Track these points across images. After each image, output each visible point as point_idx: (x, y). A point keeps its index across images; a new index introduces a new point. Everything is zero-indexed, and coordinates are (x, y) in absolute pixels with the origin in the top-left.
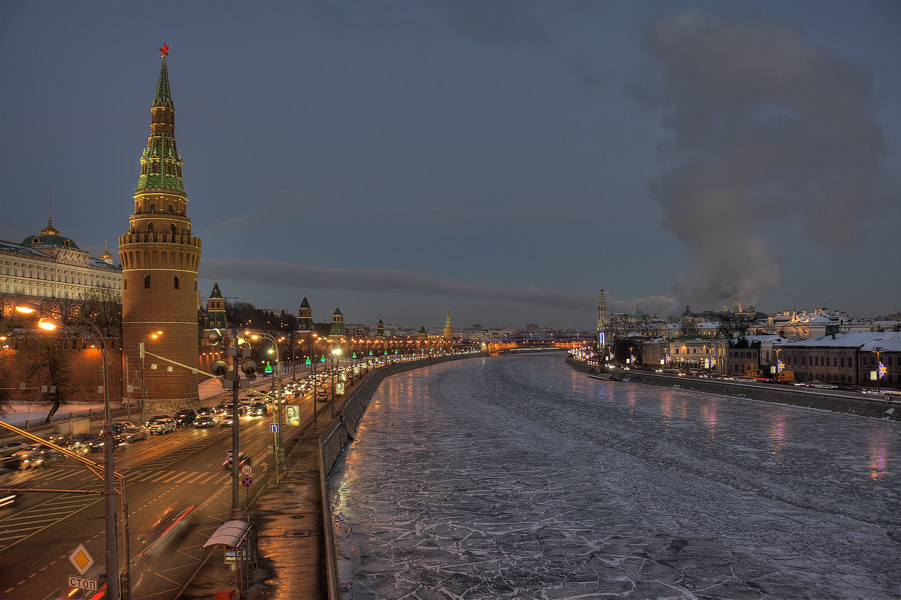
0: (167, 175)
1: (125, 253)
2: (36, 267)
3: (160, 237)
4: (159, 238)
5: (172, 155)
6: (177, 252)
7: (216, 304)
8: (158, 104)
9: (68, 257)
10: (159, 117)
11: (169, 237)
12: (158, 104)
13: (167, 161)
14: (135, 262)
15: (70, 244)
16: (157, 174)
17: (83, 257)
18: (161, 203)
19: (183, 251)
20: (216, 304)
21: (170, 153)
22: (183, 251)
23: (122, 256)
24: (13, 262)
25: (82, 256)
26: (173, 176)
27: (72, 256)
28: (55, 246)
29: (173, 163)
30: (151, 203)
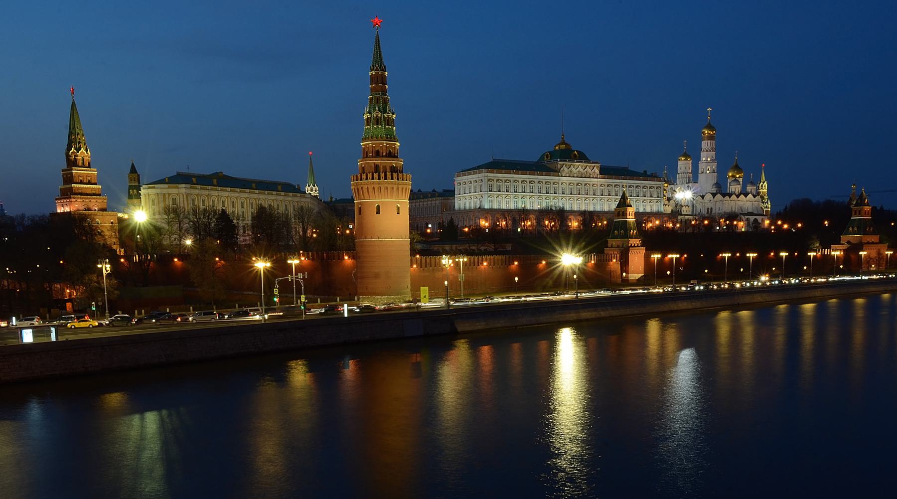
0: (375, 126)
1: (354, 189)
2: (537, 182)
3: (364, 176)
4: (363, 177)
5: (379, 110)
6: (376, 186)
8: (375, 68)
9: (574, 170)
10: (374, 79)
11: (370, 175)
12: (375, 68)
13: (375, 116)
14: (357, 197)
15: (582, 157)
16: (369, 127)
17: (592, 168)
18: (371, 150)
19: (381, 185)
21: (377, 109)
22: (381, 185)
23: (355, 191)
24: (512, 180)
25: (590, 167)
26: (380, 126)
27: (578, 167)
28: (559, 160)
29: (379, 116)
30: (377, 149)
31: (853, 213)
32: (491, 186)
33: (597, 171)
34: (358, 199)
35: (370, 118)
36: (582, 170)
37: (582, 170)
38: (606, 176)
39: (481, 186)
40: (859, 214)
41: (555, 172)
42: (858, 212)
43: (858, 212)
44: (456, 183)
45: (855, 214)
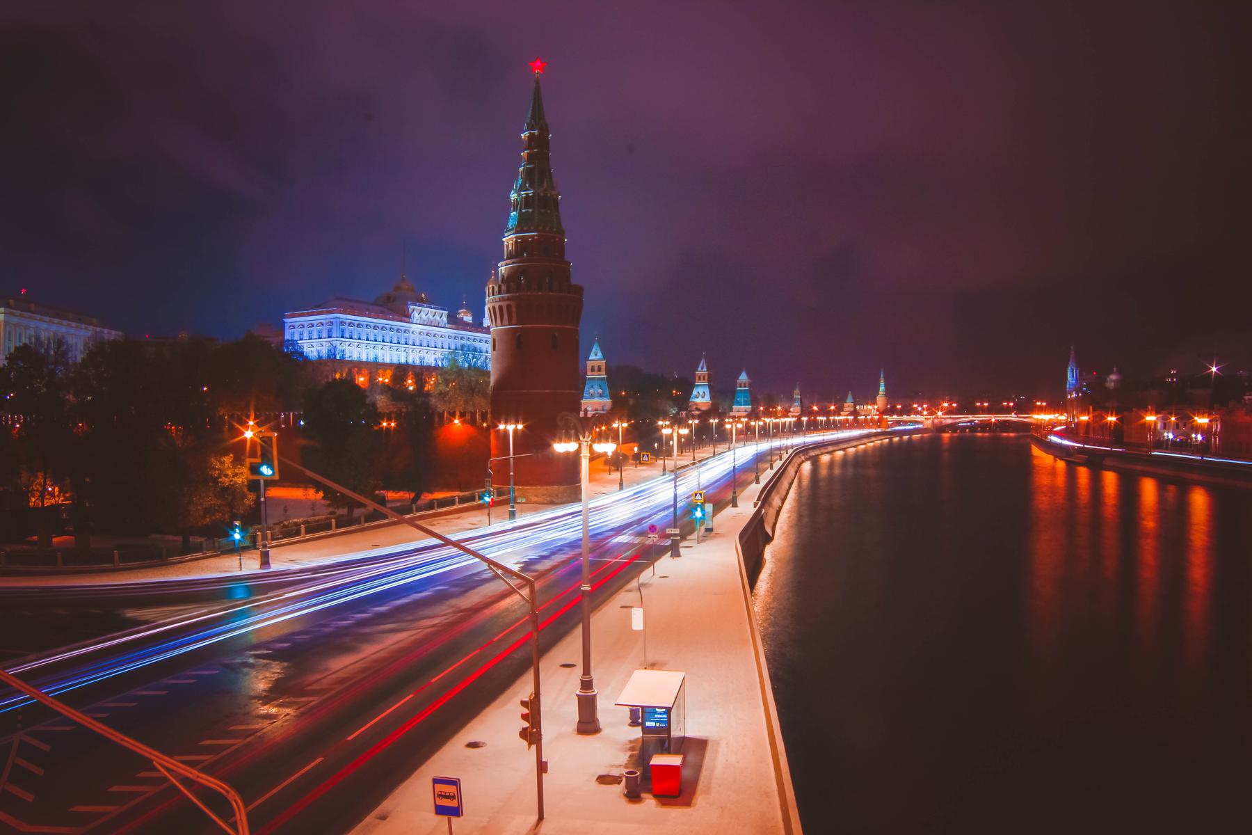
0: (543, 211)
7: (596, 368)
20: (596, 368)
26: (549, 211)
28: (409, 303)
31: (697, 378)
32: (343, 331)
33: (445, 319)
34: (514, 321)
35: (533, 197)
36: (431, 317)
37: (431, 317)
38: (454, 326)
39: (330, 331)
40: (704, 379)
41: (405, 316)
42: (702, 378)
43: (702, 378)
44: (287, 326)
45: (700, 379)
